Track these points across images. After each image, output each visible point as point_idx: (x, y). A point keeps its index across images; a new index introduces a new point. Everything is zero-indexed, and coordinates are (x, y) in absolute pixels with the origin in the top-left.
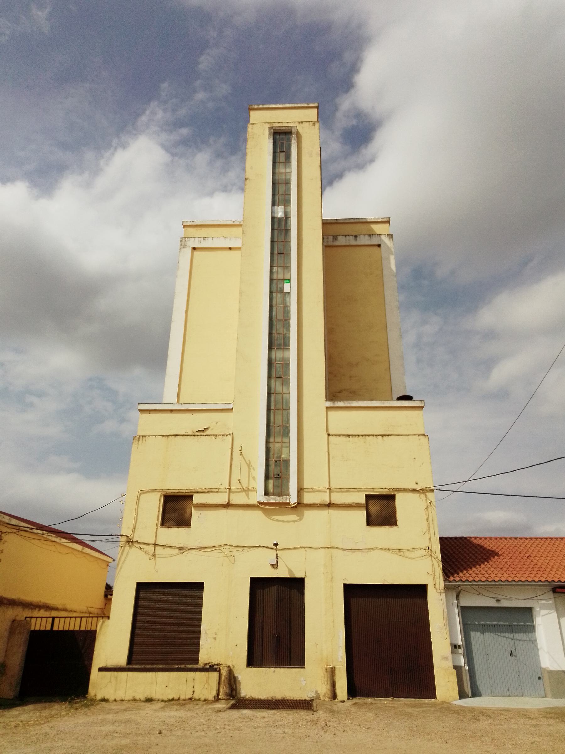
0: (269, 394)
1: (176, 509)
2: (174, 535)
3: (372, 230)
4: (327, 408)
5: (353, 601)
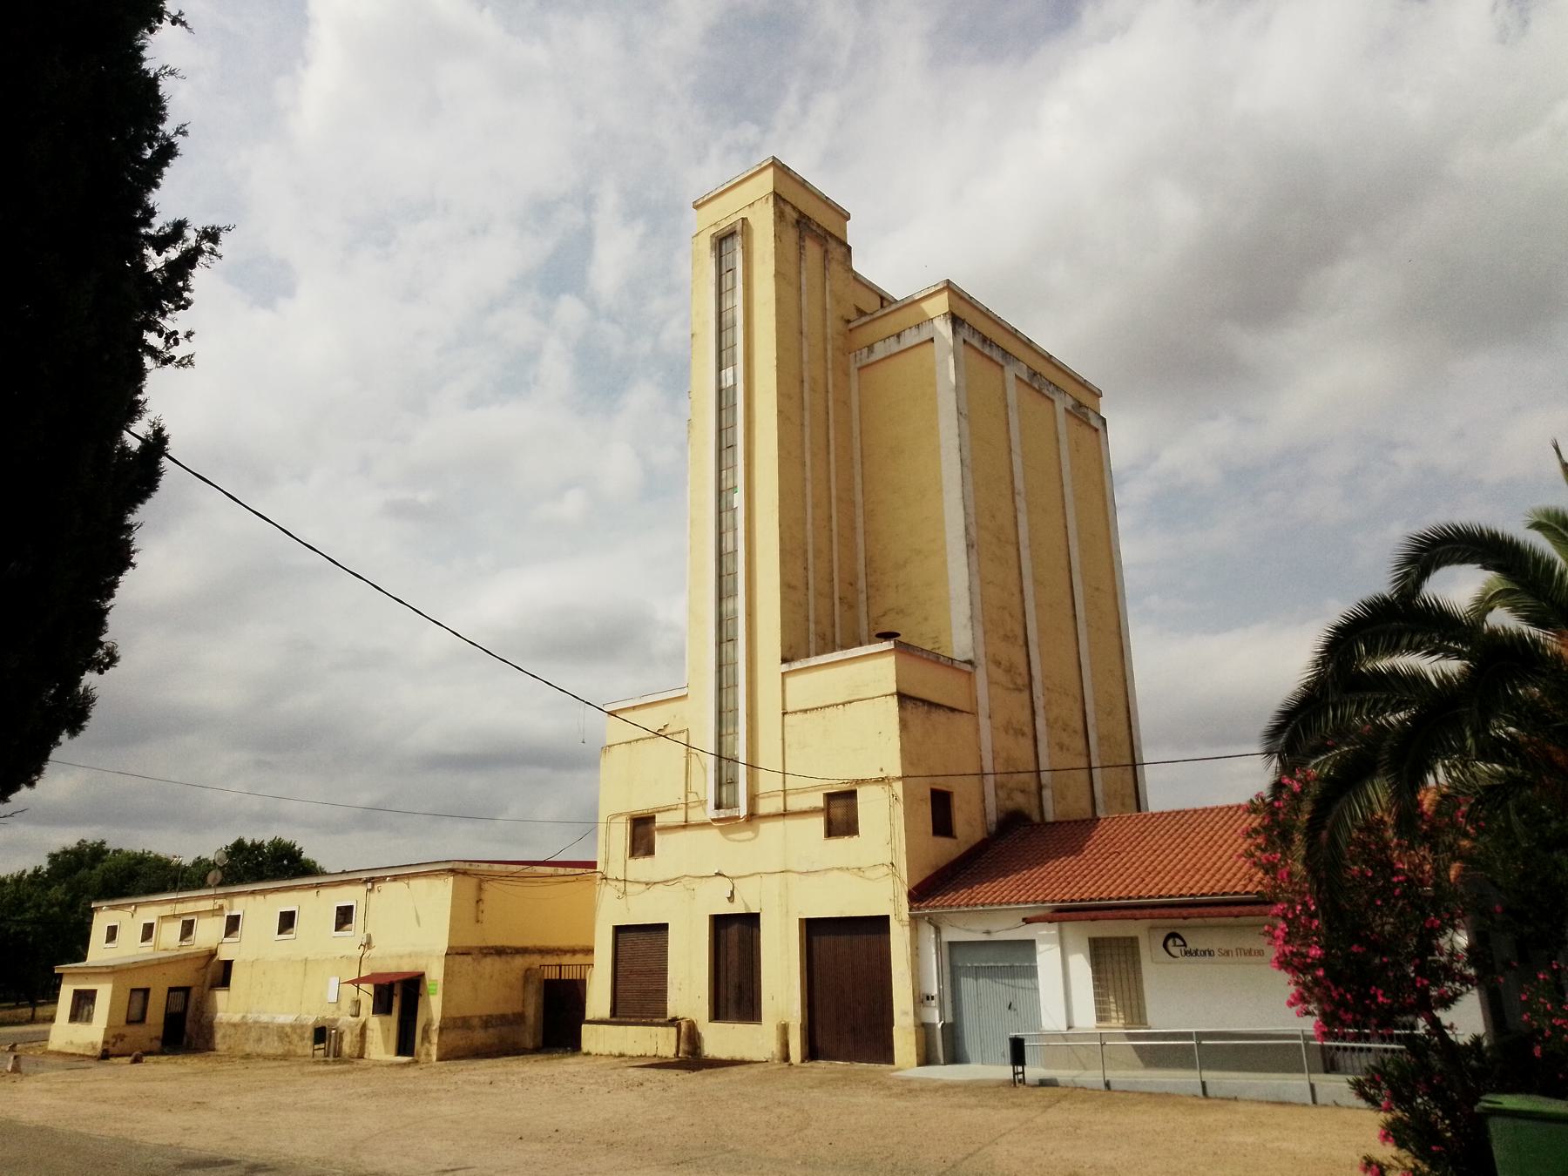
1: (642, 833)
2: (641, 867)
3: (923, 313)
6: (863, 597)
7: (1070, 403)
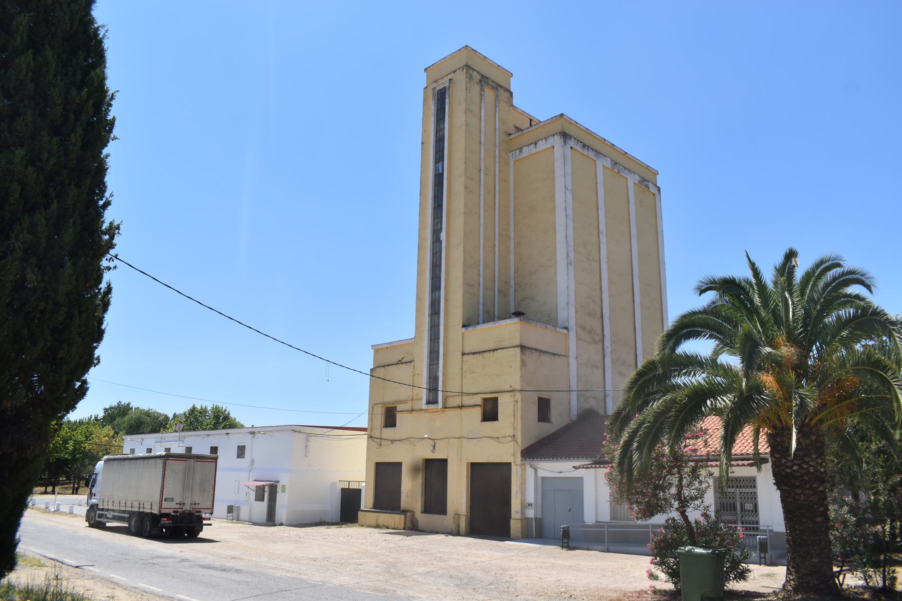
2: (389, 432)
6: (512, 290)
7: (637, 178)
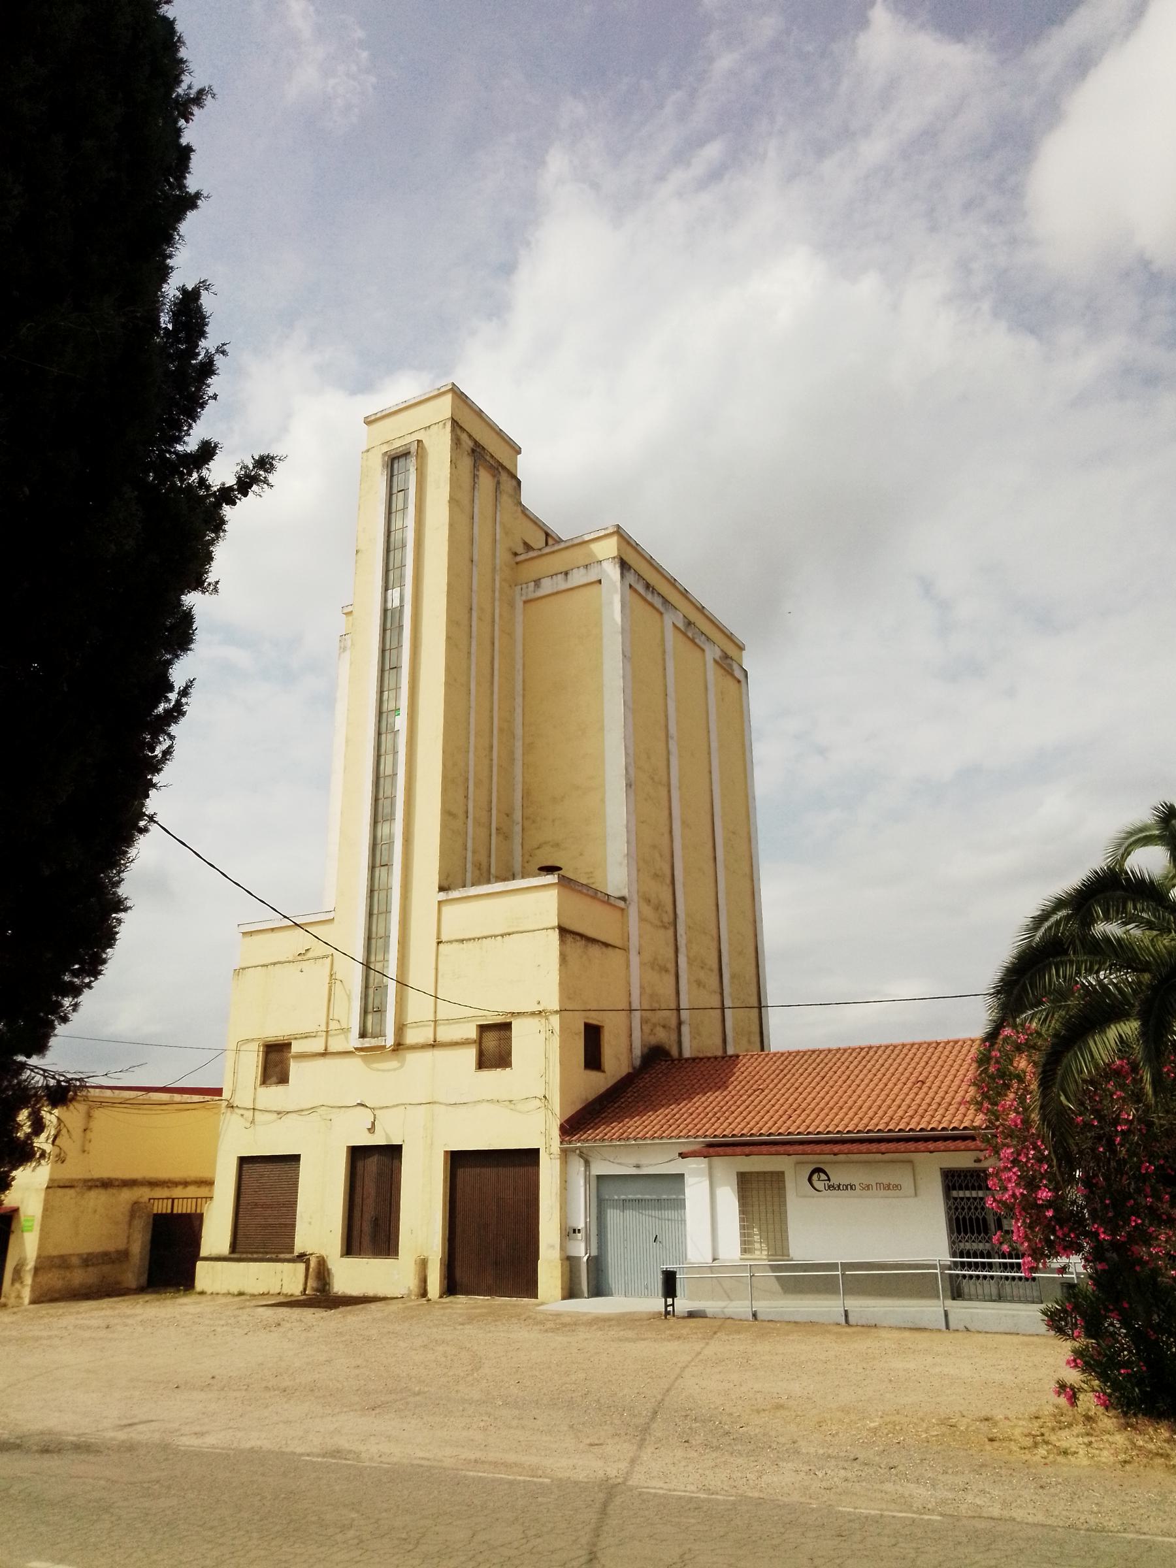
0: (371, 891)
1: (276, 1060)
2: (274, 1095)
3: (591, 554)
4: (439, 902)
5: (460, 1172)
6: (518, 829)
7: (718, 654)
